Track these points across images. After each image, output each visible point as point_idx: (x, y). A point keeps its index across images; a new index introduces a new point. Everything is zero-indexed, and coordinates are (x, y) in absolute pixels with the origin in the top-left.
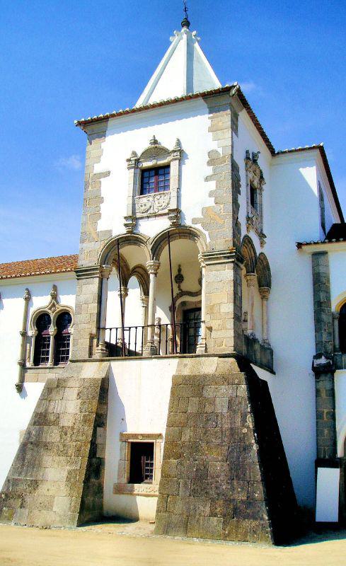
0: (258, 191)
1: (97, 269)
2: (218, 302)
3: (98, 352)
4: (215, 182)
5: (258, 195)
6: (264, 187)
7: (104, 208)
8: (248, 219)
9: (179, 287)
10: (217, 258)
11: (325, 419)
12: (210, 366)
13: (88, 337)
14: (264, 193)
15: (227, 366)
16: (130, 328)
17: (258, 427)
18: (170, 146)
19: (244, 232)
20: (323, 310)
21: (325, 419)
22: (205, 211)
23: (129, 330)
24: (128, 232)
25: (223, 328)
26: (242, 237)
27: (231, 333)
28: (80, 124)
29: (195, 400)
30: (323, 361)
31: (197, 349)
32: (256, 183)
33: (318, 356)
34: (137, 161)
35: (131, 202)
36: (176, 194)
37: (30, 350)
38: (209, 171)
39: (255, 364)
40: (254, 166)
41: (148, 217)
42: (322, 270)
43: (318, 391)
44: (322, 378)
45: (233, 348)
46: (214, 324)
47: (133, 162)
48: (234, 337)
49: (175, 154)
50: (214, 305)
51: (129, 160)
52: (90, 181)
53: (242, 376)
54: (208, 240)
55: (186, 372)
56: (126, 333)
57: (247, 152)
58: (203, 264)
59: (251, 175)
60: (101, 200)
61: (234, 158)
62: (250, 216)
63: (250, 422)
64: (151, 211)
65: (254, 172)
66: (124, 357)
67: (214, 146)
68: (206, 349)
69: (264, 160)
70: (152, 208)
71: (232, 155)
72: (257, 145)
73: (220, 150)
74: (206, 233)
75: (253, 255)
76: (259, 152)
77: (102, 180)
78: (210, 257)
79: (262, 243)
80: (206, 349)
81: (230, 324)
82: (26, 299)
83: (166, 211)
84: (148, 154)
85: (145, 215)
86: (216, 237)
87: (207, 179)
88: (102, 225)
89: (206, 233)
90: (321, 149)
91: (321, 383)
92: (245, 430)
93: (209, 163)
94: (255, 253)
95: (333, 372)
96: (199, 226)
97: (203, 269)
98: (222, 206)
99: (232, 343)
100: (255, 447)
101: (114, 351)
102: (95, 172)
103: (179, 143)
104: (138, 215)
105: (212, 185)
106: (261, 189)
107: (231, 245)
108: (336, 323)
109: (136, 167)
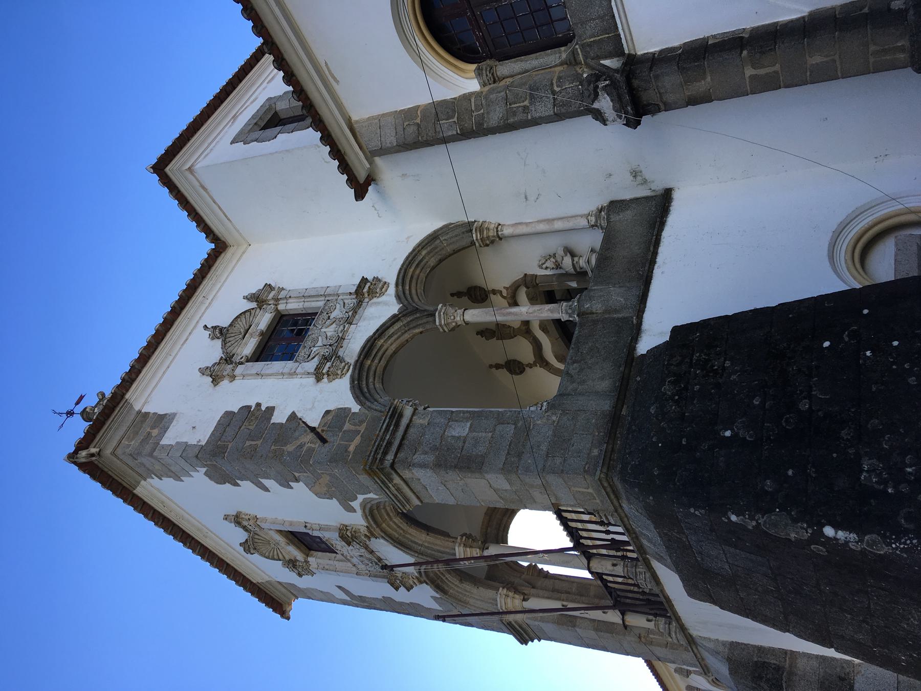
9: (530, 366)
11: (777, 67)
20: (480, 124)
21: (777, 67)
30: (605, 103)
32: (264, 320)
33: (599, 116)
39: (636, 331)
42: (390, 139)
43: (693, 101)
44: (649, 96)
69: (225, 300)
73: (204, 470)
75: (396, 327)
76: (206, 327)
90: (160, 168)
91: (670, 98)
95: (633, 63)
108: (505, 68)
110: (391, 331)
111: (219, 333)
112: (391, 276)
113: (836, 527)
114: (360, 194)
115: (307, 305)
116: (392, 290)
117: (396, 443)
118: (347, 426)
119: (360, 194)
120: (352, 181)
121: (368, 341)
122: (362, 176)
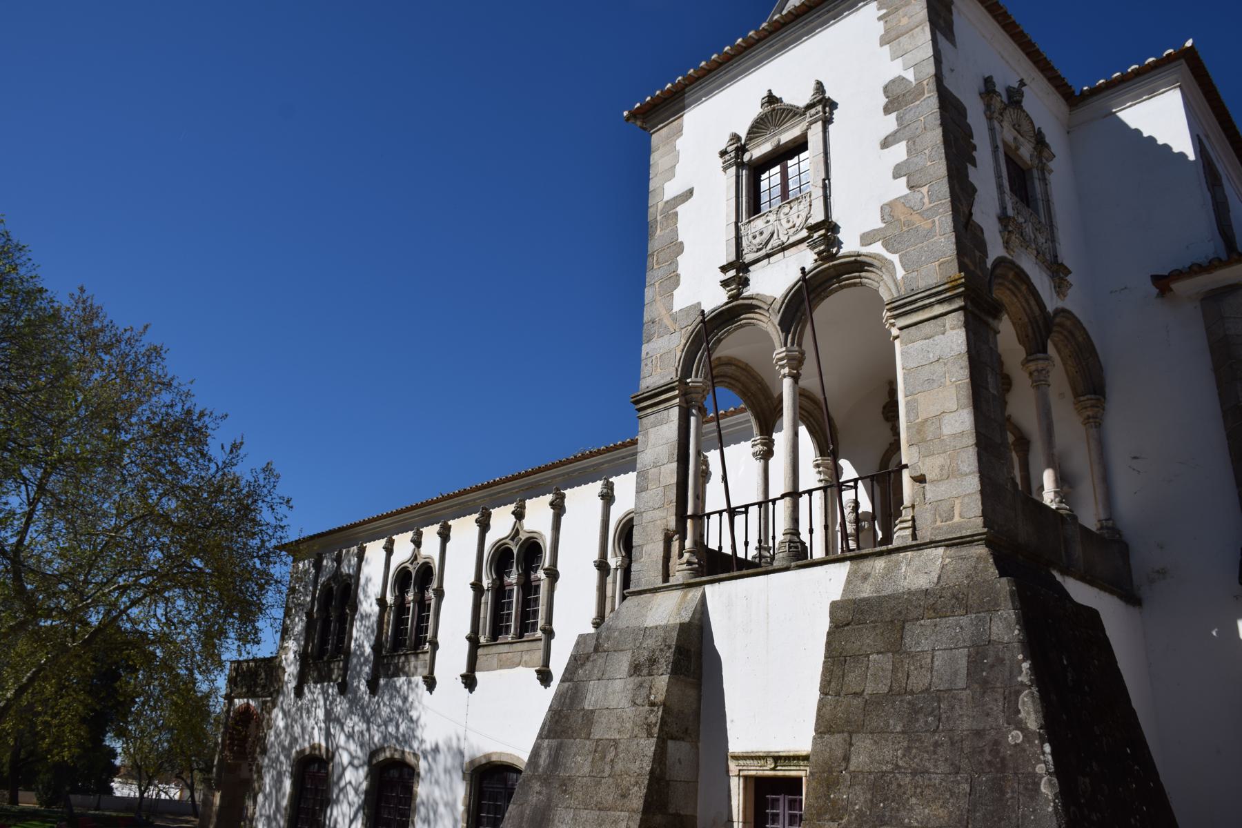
0: (1036, 173)
1: (673, 389)
2: (934, 410)
3: (679, 573)
4: (904, 143)
5: (1037, 183)
6: (1052, 165)
7: (685, 264)
8: (1003, 219)
10: (923, 307)
12: (917, 572)
13: (661, 537)
14: (1053, 179)
15: (966, 566)
16: (747, 507)
18: (797, 95)
19: (996, 249)
22: (889, 211)
23: (746, 512)
24: (733, 298)
25: (950, 474)
26: (989, 265)
27: (972, 484)
28: (634, 115)
32: (1026, 151)
34: (742, 150)
35: (733, 234)
36: (820, 192)
37: (614, 597)
38: (890, 123)
39: (1065, 572)
40: (1010, 114)
41: (768, 256)
45: (980, 521)
46: (930, 467)
47: (733, 154)
49: (813, 111)
50: (926, 420)
51: (723, 153)
53: (1004, 585)
54: (900, 273)
55: (866, 591)
56: (740, 520)
57: (988, 81)
58: (895, 332)
59: (1008, 134)
60: (679, 248)
61: (946, 83)
62: (1010, 212)
63: (1030, 714)
64: (774, 242)
65: (1016, 127)
66: (736, 573)
67: (895, 69)
68: (914, 527)
70: (775, 236)
71: (939, 78)
72: (1009, 66)
73: (910, 75)
74: (895, 258)
77: (680, 209)
78: (902, 307)
79: (1060, 286)
80: (914, 527)
81: (968, 461)
82: (603, 496)
83: (804, 233)
84: (759, 128)
85: (763, 252)
86: (917, 261)
87: (885, 144)
88: (682, 299)
89: (895, 258)
92: (1015, 737)
93: (887, 110)
94: (1042, 306)
96: (877, 248)
97: (897, 342)
98: (925, 190)
99: (976, 507)
100: (1047, 789)
101: (718, 566)
102: (666, 198)
103: (820, 87)
104: (748, 257)
105: (899, 152)
106: (1043, 170)
107: (953, 271)
109: (740, 165)
110: (1033, 303)
111: (1015, 98)
112: (1073, 302)
113: (1053, 753)
114: (1156, 279)
115: (1040, 203)
116: (1060, 304)
117: (977, 312)
118: (978, 254)
119: (1156, 279)
120: (1178, 275)
121: (1027, 277)
122: (1178, 287)
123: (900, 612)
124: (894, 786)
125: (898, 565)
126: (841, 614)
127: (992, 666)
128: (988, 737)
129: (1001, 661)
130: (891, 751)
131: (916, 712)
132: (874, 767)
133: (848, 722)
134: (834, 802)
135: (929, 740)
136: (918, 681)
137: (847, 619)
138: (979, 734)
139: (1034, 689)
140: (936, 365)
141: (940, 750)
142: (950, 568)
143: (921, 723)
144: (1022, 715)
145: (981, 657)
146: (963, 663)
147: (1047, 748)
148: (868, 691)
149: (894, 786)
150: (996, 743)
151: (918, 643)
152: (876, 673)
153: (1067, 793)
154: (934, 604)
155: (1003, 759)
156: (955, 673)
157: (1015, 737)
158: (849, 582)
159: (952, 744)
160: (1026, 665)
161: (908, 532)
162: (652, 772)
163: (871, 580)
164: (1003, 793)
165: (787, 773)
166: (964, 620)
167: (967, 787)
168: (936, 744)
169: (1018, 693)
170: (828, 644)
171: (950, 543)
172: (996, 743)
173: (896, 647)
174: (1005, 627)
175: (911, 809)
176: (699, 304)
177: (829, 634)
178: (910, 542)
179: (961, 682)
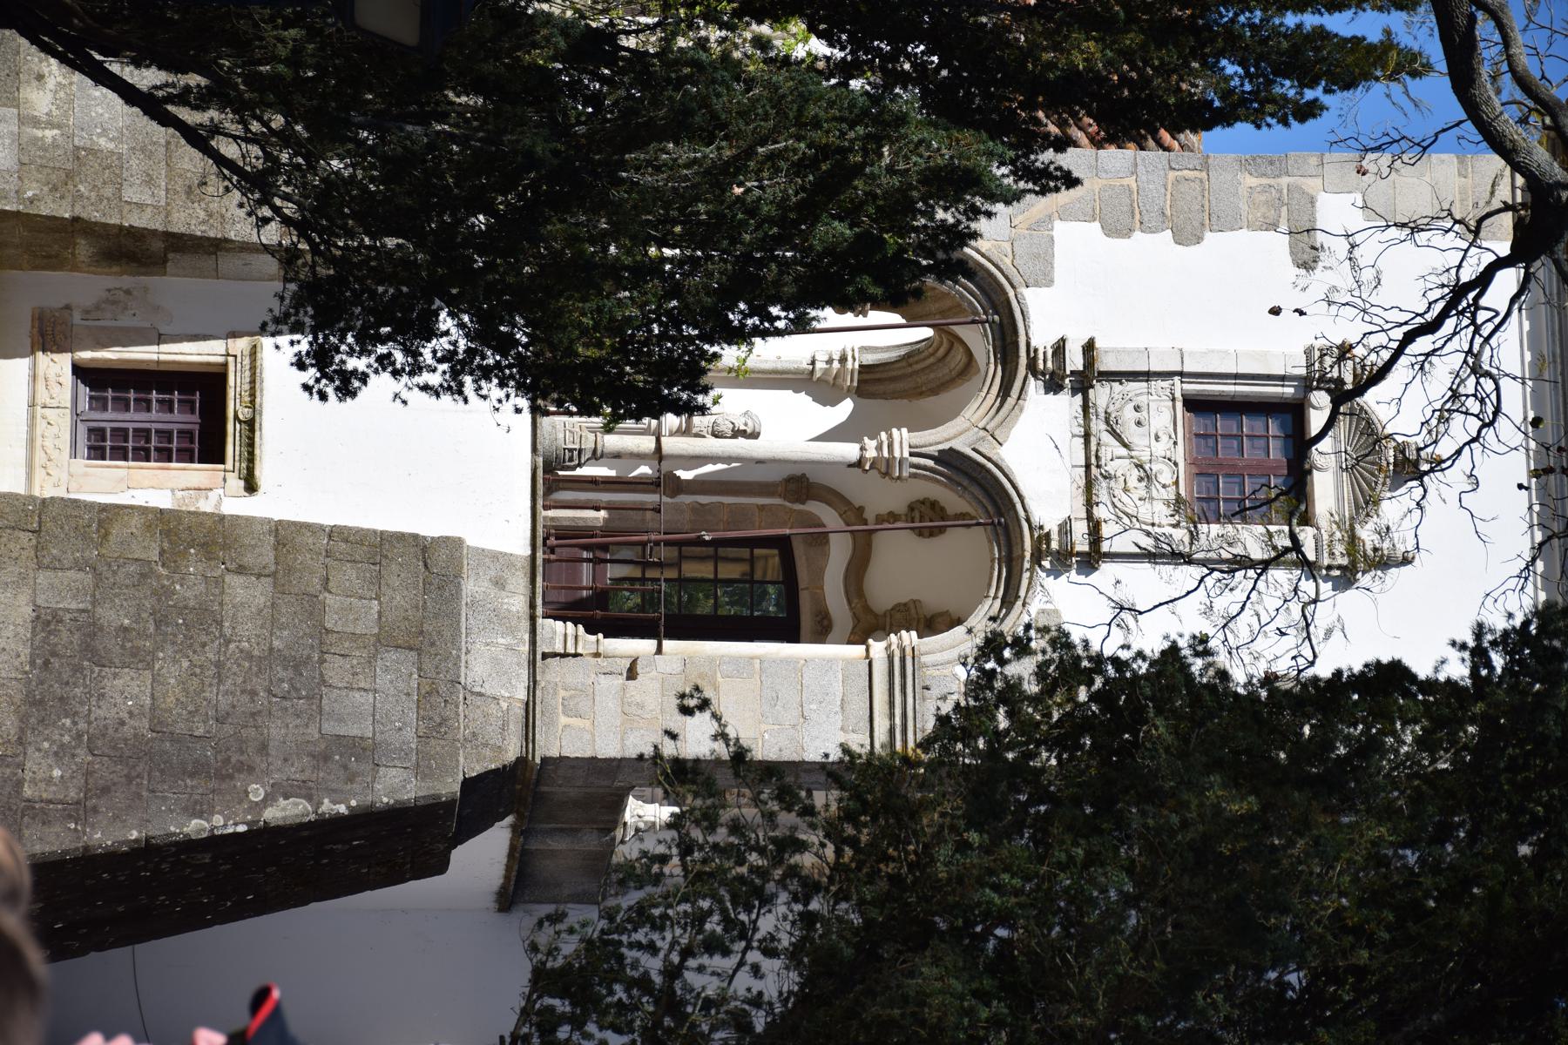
12: (492, 663)
15: (491, 733)
17: (265, 838)
27: (608, 748)
29: (367, 625)
31: (559, 624)
41: (1087, 436)
45: (554, 753)
48: (594, 759)
49: (1339, 548)
52: (1285, 180)
55: (472, 586)
64: (1110, 448)
68: (564, 655)
70: (1124, 452)
80: (564, 655)
85: (1098, 426)
92: (257, 792)
99: (575, 748)
100: (195, 827)
113: (235, 835)
123: (433, 644)
124: (204, 638)
125: (511, 631)
126: (442, 555)
127: (345, 767)
128: (258, 760)
129: (351, 779)
130: (247, 634)
131: (296, 668)
132: (228, 610)
133: (290, 570)
134: (185, 553)
135: (259, 684)
136: (336, 670)
137: (432, 563)
138: (263, 748)
139: (312, 817)
140: (797, 713)
141: (245, 698)
142: (493, 709)
143: (282, 674)
144: (282, 802)
145: (362, 753)
146: (353, 730)
147: (242, 828)
148: (330, 599)
149: (204, 638)
150: (251, 769)
151: (387, 670)
152: (352, 609)
153: (190, 846)
154: (439, 691)
155: (231, 777)
156: (341, 720)
157: (257, 792)
158: (496, 556)
159: (253, 715)
160: (342, 809)
161: (559, 648)
162: (226, 240)
163: (493, 592)
164: (192, 775)
165: (230, 439)
166: (409, 734)
167: (200, 732)
168: (253, 694)
169: (309, 798)
170: (401, 537)
171: (529, 708)
172: (251, 769)
173: (384, 640)
174: (395, 785)
175: (175, 661)
176: (1049, 282)
177: (415, 537)
178: (542, 648)
179: (330, 727)
